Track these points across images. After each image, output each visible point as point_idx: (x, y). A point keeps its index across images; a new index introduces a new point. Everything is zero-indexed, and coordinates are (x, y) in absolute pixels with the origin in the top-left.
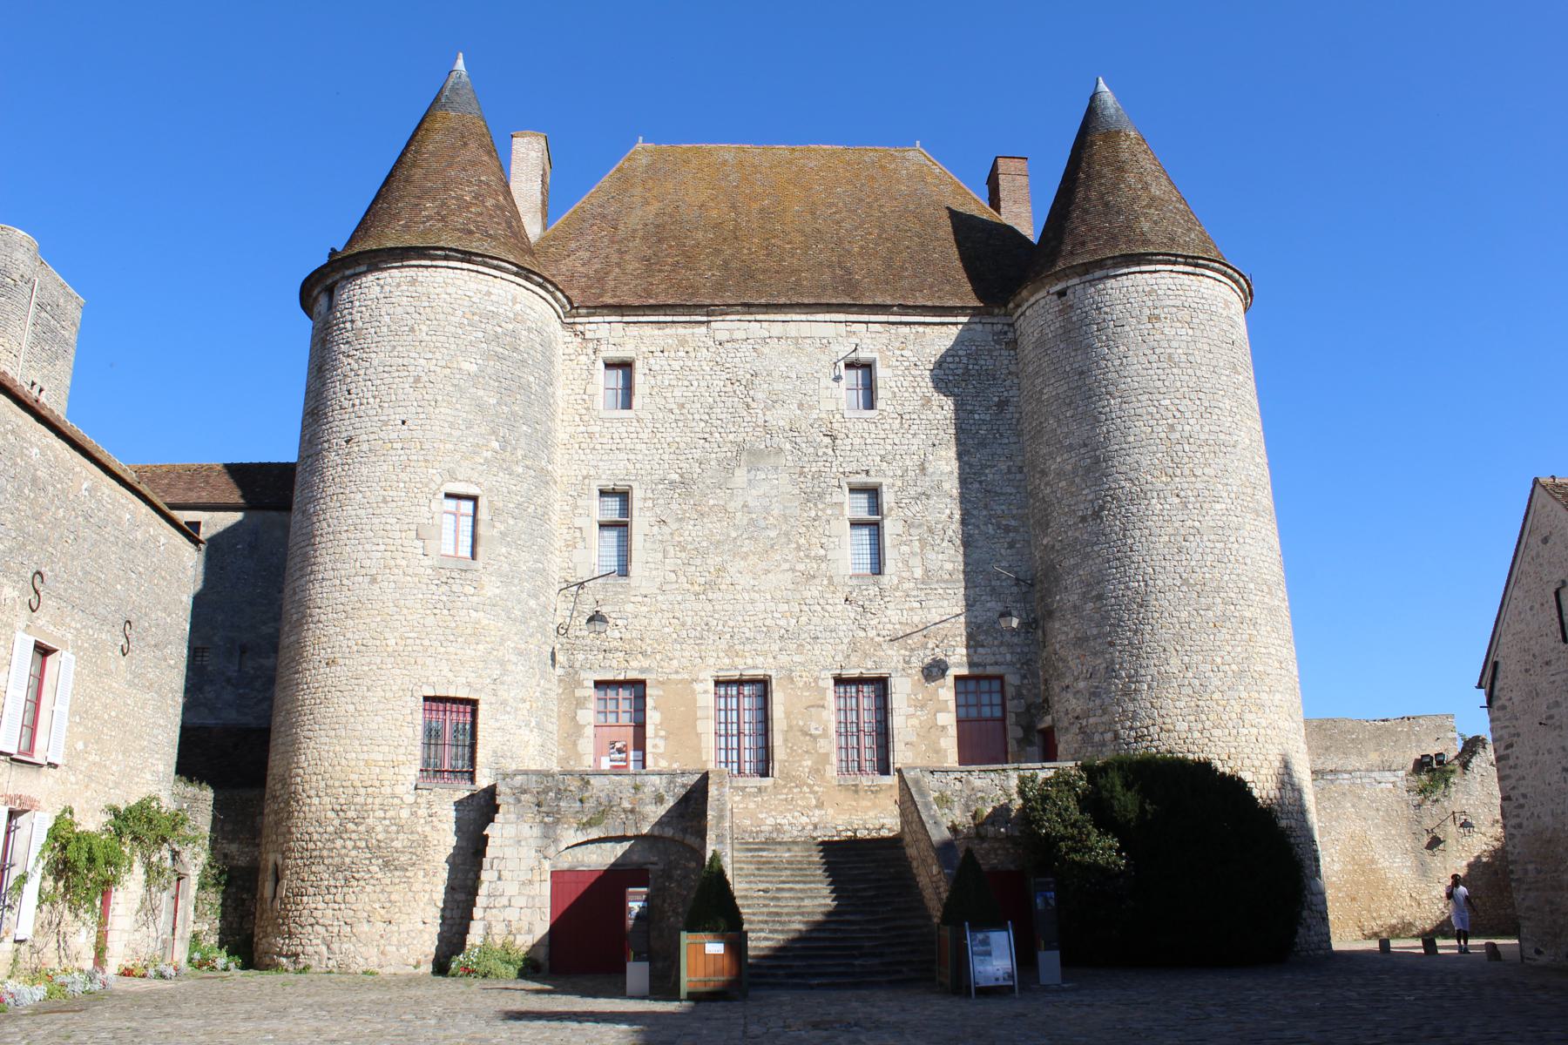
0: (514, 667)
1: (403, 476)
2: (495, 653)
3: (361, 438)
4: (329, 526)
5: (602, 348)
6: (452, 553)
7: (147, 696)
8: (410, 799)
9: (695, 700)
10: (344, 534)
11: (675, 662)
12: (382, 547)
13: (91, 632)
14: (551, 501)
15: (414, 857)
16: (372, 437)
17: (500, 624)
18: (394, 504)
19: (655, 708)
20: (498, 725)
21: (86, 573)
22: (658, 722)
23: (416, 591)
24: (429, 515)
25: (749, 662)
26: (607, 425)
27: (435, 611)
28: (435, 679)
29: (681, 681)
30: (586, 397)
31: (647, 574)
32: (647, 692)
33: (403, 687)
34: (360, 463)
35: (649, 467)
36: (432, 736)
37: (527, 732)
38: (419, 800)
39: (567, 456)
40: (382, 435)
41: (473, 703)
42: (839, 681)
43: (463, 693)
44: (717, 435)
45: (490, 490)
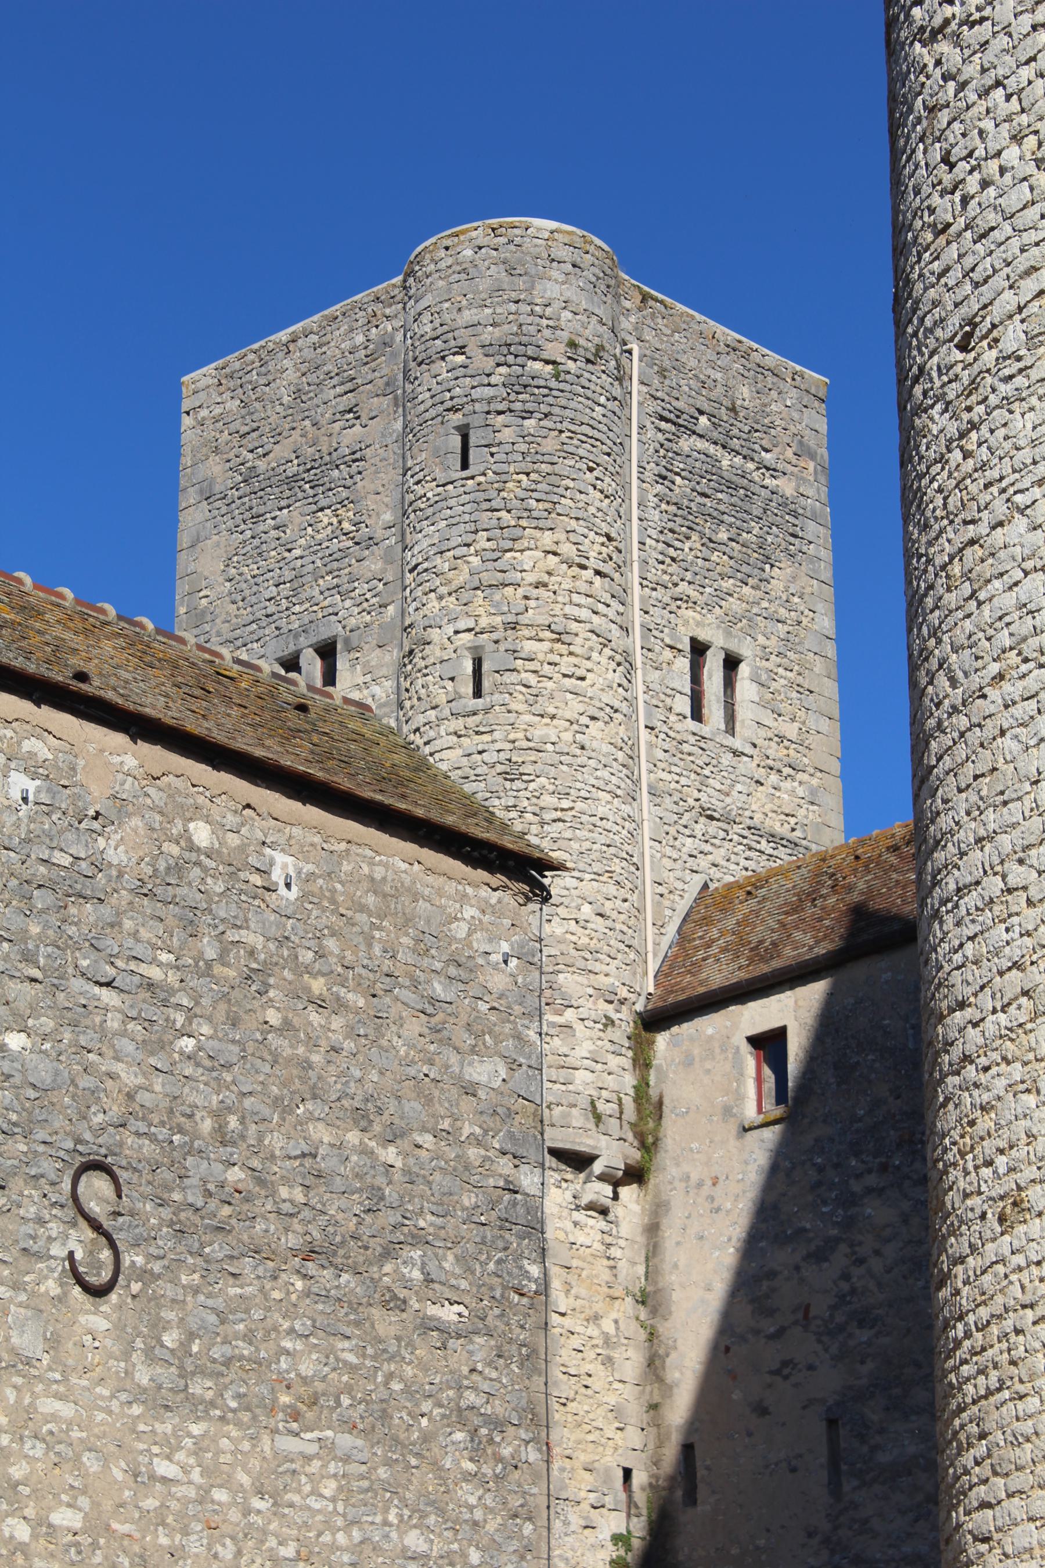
3: (996, 313)
4: (954, 682)
7: (289, 1444)
10: (992, 693)
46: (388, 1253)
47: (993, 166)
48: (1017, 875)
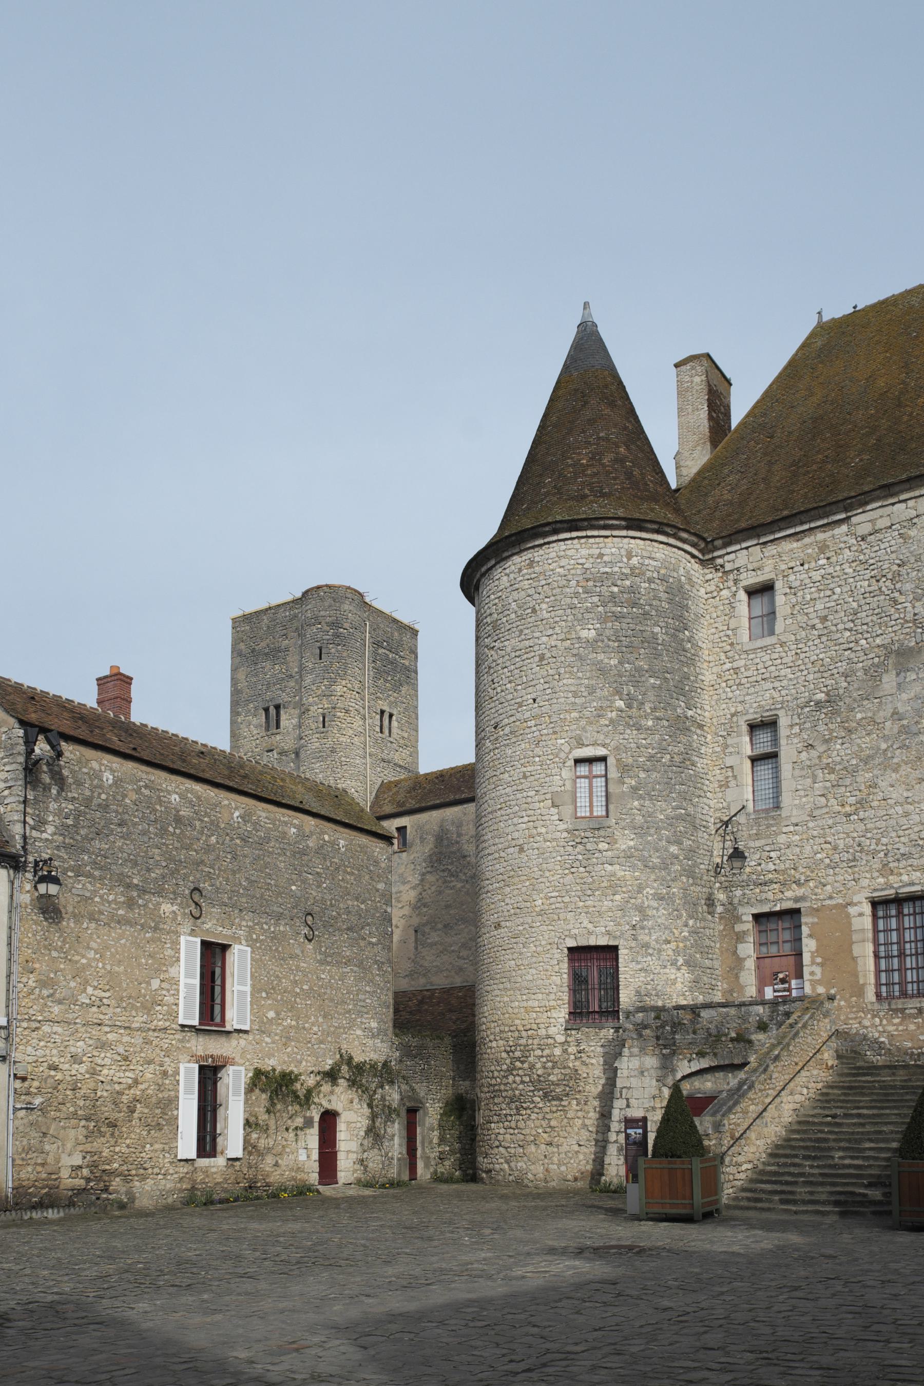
0: (655, 911)
1: (538, 751)
2: (633, 901)
3: (504, 723)
5: (742, 577)
6: (588, 814)
7: (345, 970)
8: (561, 1038)
9: (850, 924)
11: (829, 887)
12: (526, 819)
13: (265, 927)
14: (695, 745)
15: (568, 1089)
16: (512, 719)
17: (637, 874)
18: (532, 778)
19: (810, 936)
20: (640, 966)
21: (251, 882)
22: (814, 949)
23: (555, 855)
24: (561, 783)
25: (905, 878)
26: (751, 656)
27: (573, 870)
28: (576, 931)
29: (837, 906)
30: (729, 632)
31: (797, 802)
32: (803, 920)
33: (550, 941)
34: (504, 745)
35: (794, 691)
36: (578, 981)
37: (674, 971)
38: (569, 1039)
39: (715, 697)
40: (518, 716)
41: (614, 949)
43: (602, 941)
44: (863, 642)
45: (617, 748)
46: (362, 928)
47: (504, 687)
48: (502, 854)
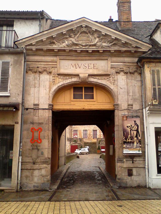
42: (93, 130)
